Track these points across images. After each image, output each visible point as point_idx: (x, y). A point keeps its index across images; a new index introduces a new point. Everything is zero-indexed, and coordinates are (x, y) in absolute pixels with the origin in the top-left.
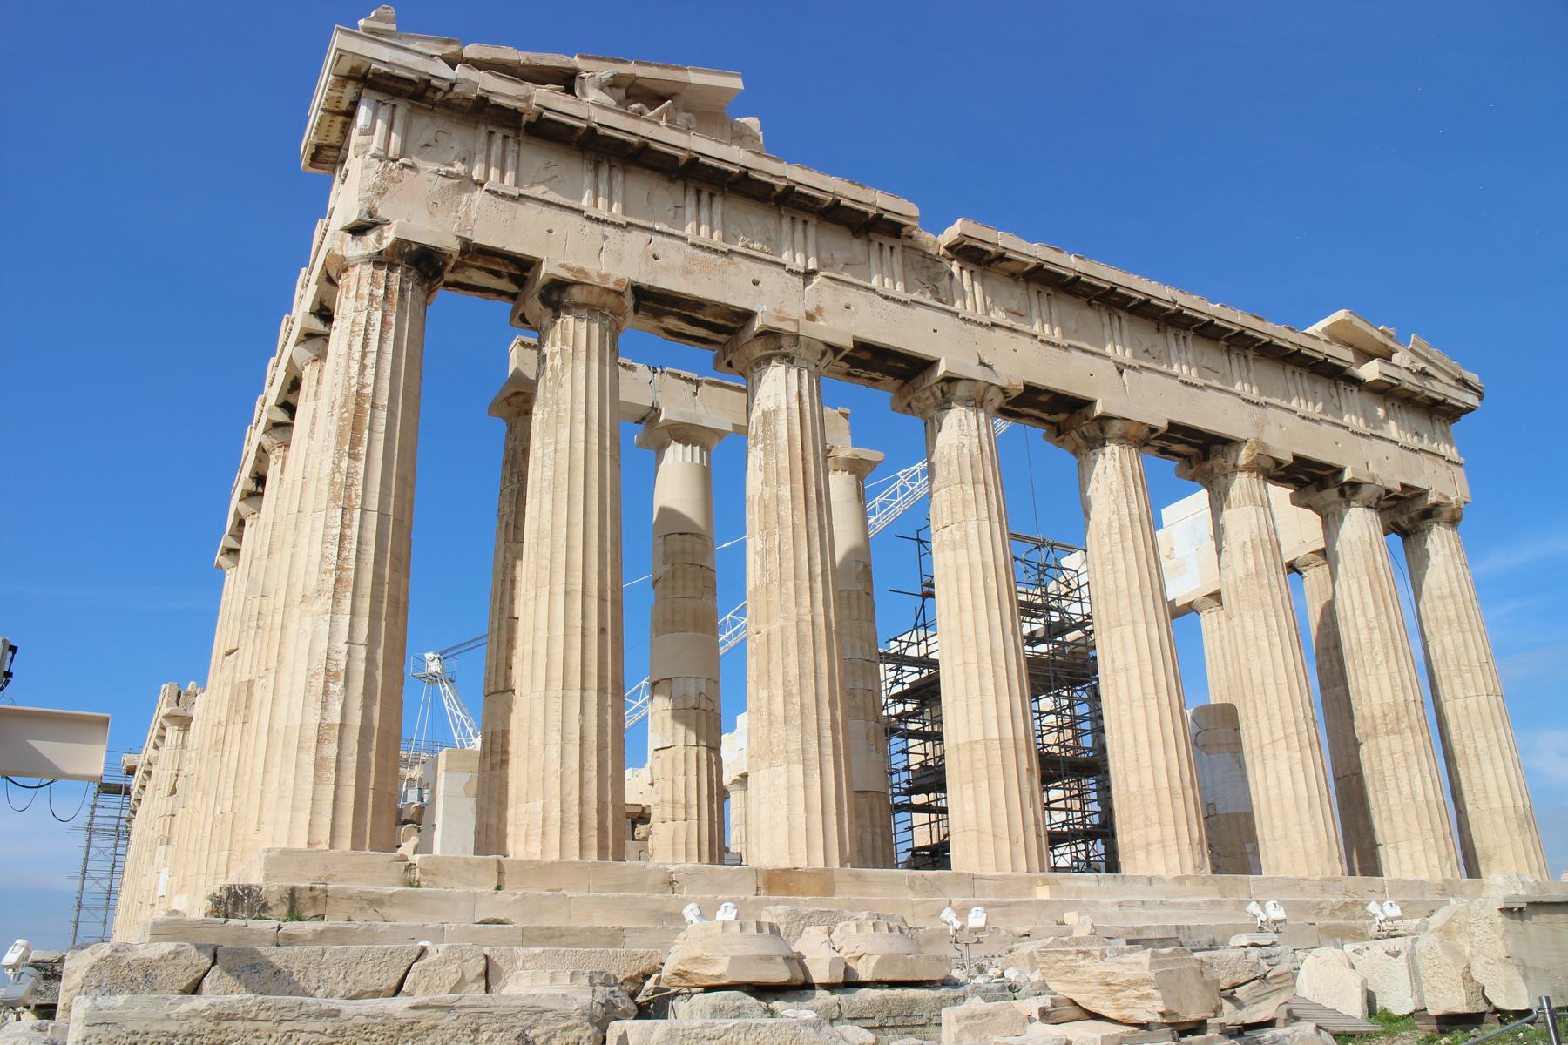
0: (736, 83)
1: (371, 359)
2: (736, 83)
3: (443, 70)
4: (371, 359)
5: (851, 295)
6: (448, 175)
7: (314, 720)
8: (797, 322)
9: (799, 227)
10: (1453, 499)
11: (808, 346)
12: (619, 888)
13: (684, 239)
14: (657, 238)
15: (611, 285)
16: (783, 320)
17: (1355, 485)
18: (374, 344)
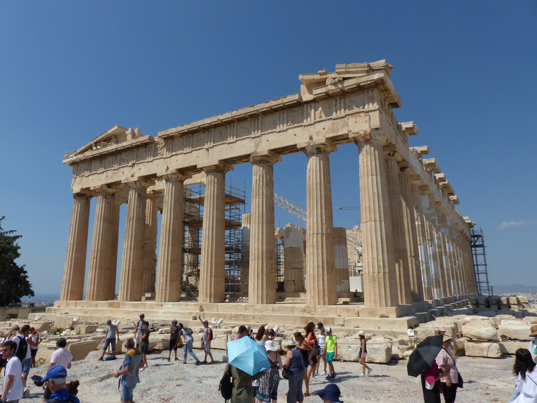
0: (116, 127)
2: (116, 127)
3: (75, 158)
5: (141, 166)
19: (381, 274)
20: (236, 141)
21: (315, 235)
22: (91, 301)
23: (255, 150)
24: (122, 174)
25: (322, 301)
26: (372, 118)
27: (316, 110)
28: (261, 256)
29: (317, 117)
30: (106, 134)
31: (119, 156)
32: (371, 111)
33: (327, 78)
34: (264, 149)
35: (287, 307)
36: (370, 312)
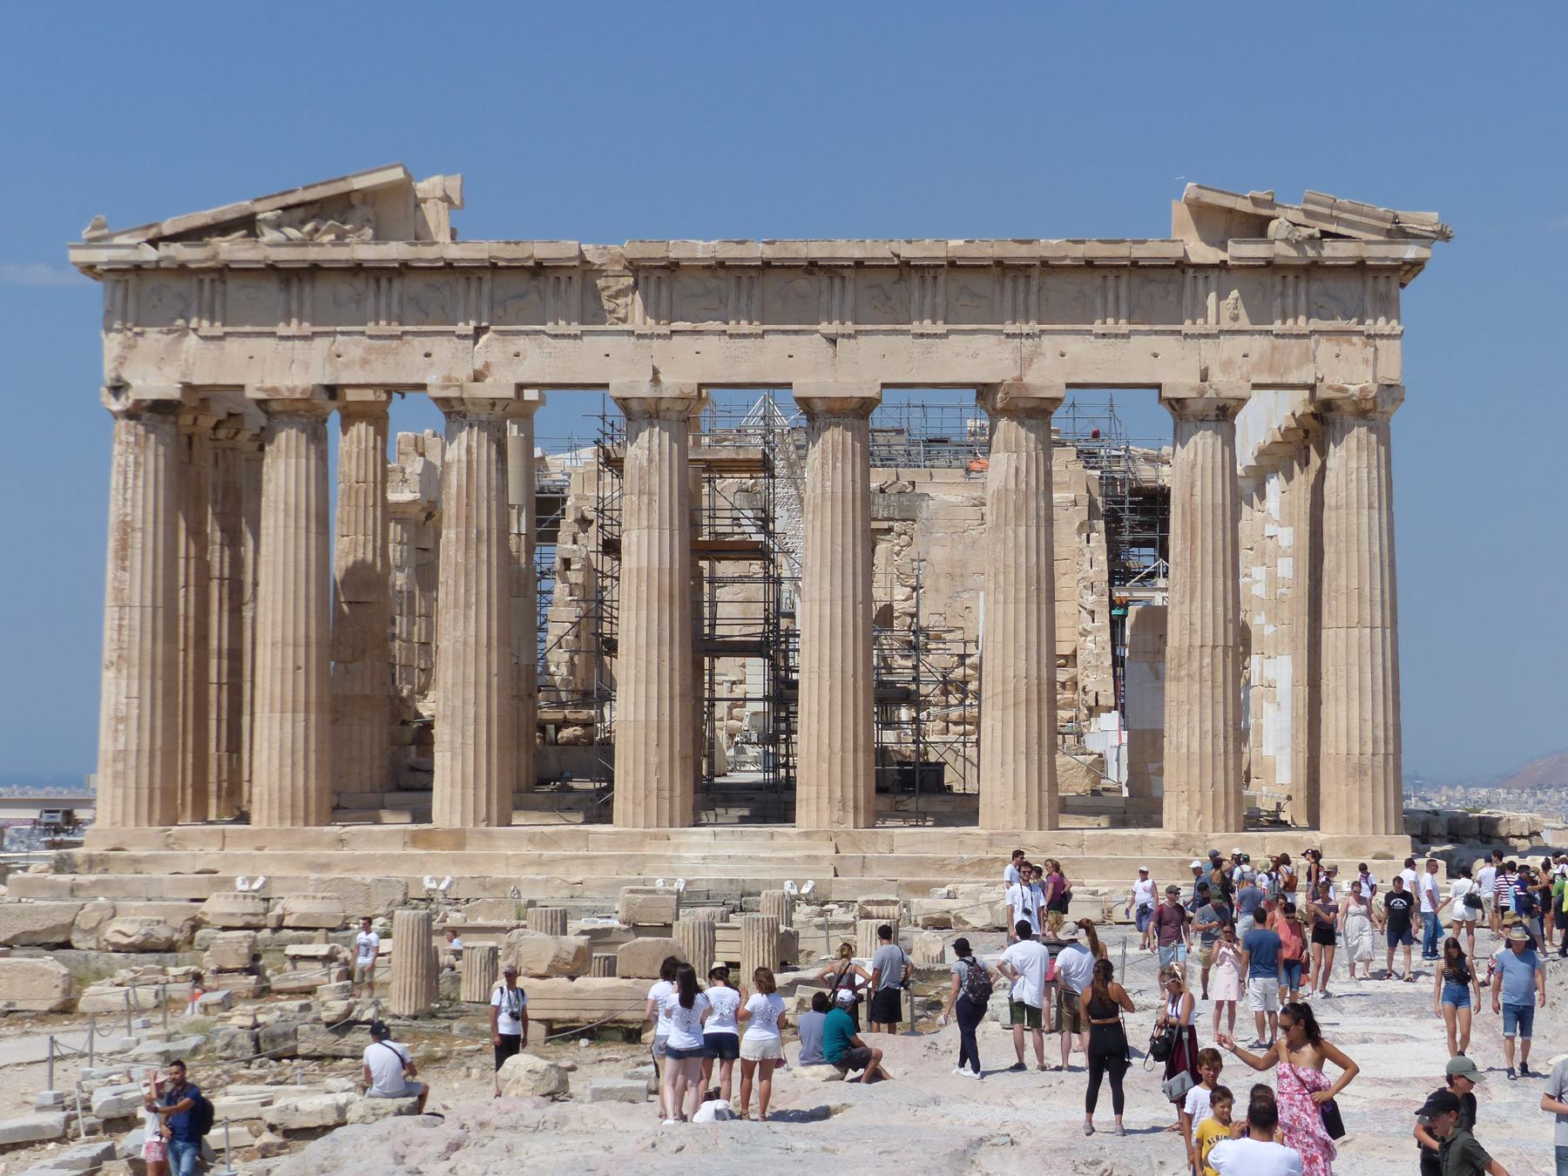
1: (130, 492)
2: (397, 174)
4: (129, 495)
5: (521, 343)
6: (169, 332)
7: (111, 748)
8: (461, 386)
9: (474, 283)
10: (1354, 389)
11: (474, 404)
12: (304, 845)
13: (363, 333)
14: (339, 337)
15: (298, 396)
16: (447, 388)
17: (1178, 400)
18: (130, 482)
19: (1380, 758)
20: (949, 333)
21: (1208, 650)
22: (300, 826)
23: (1016, 374)
24: (420, 359)
25: (1222, 822)
26: (1381, 354)
27: (1222, 296)
28: (1034, 697)
29: (1226, 314)
30: (342, 187)
31: (397, 284)
32: (1382, 336)
33: (1271, 218)
34: (1046, 377)
35: (1123, 837)
36: (1351, 848)
